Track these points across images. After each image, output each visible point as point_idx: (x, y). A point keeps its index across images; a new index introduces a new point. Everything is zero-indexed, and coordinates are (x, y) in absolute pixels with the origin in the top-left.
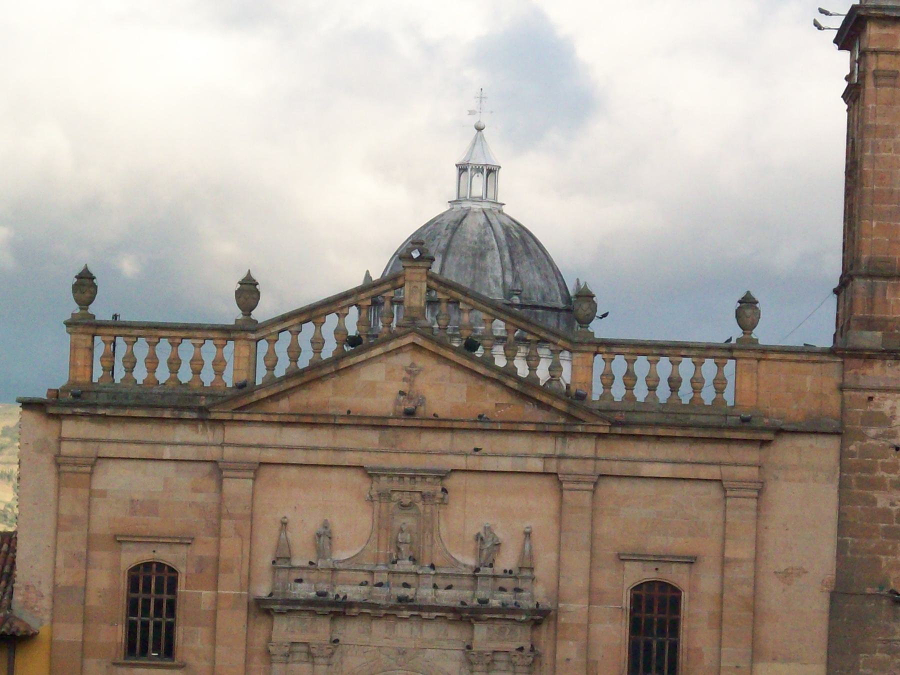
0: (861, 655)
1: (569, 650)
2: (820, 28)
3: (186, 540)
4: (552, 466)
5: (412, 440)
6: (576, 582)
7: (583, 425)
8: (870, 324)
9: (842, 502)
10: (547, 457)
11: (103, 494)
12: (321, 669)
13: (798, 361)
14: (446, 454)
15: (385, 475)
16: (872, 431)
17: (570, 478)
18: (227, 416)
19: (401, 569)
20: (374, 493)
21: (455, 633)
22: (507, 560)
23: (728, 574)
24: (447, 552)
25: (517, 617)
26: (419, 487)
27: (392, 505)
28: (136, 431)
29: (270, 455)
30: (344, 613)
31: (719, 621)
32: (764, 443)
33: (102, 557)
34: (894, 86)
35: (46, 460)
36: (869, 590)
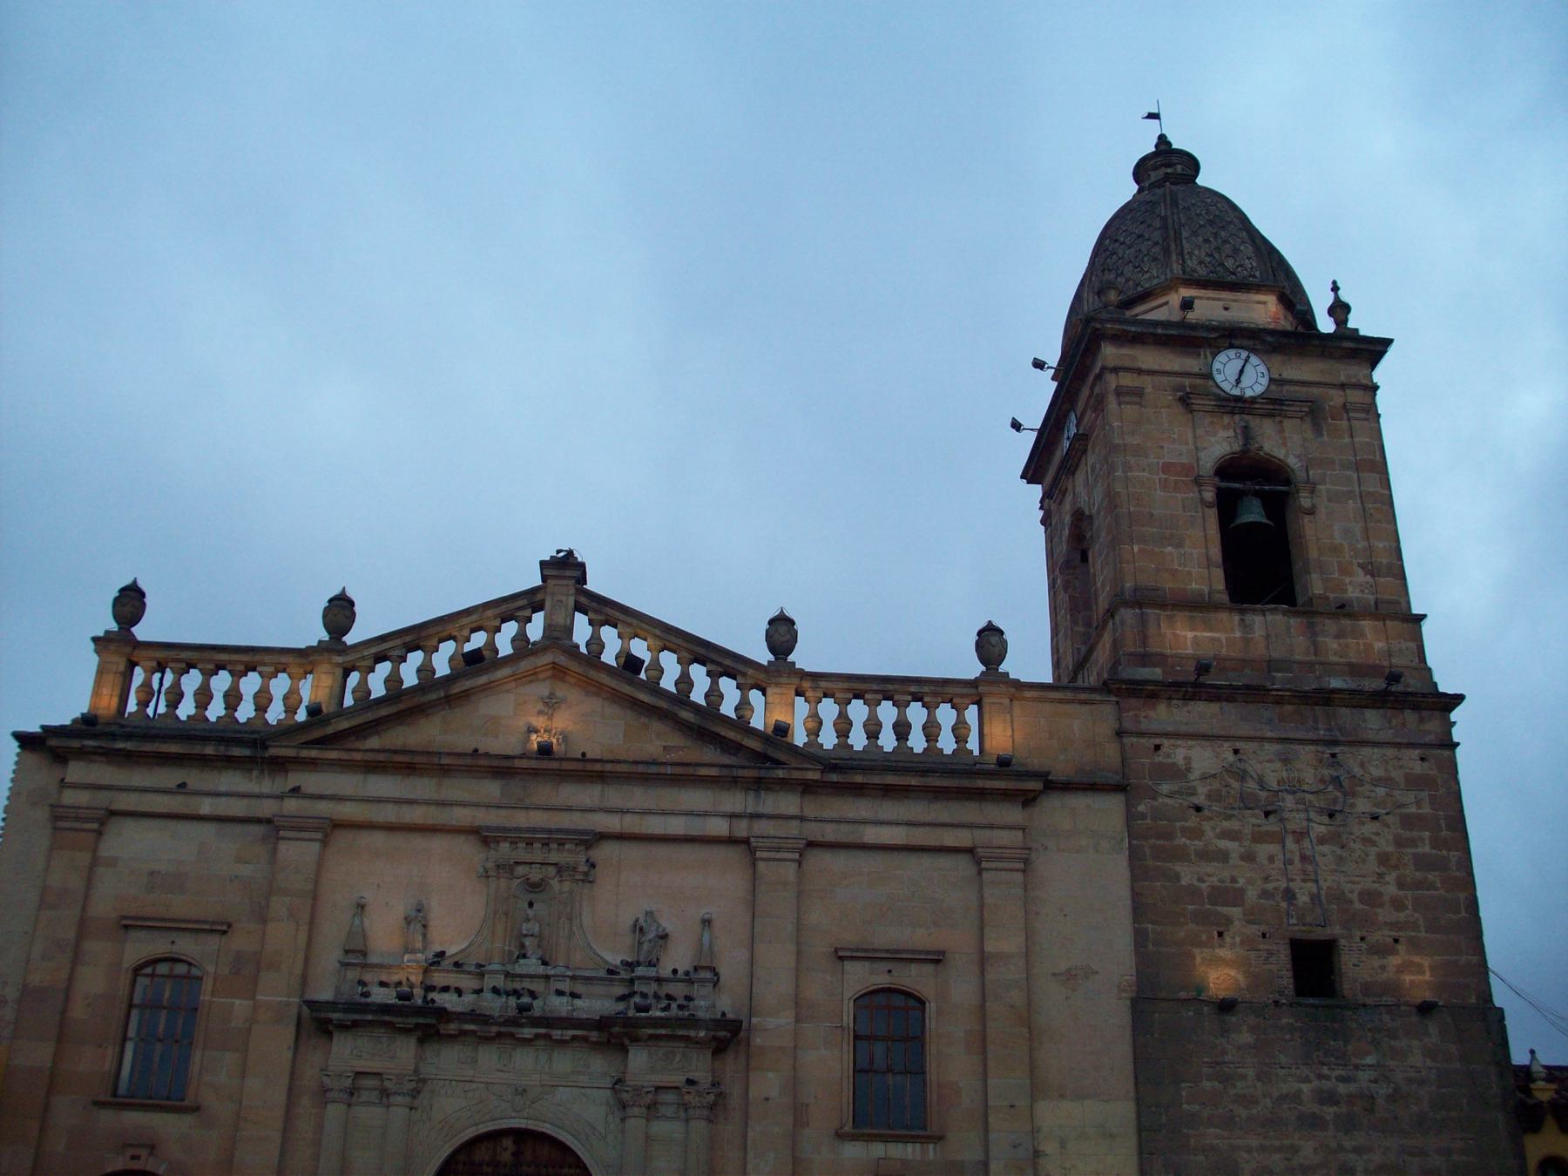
0: (1183, 1085)
1: (768, 1084)
3: (222, 929)
4: (742, 828)
5: (545, 793)
6: (776, 983)
7: (783, 768)
8: (1145, 659)
9: (1135, 876)
10: (733, 816)
11: (113, 863)
12: (399, 1114)
13: (1061, 701)
14: (591, 810)
15: (505, 839)
16: (1165, 788)
18: (291, 753)
19: (524, 971)
20: (490, 865)
21: (599, 1065)
22: (678, 958)
23: (988, 977)
24: (591, 948)
25: (692, 1033)
26: (554, 857)
27: (516, 882)
28: (168, 777)
29: (348, 811)
30: (438, 1032)
31: (981, 1042)
32: (1028, 800)
33: (96, 948)
35: (42, 814)
36: (1183, 995)
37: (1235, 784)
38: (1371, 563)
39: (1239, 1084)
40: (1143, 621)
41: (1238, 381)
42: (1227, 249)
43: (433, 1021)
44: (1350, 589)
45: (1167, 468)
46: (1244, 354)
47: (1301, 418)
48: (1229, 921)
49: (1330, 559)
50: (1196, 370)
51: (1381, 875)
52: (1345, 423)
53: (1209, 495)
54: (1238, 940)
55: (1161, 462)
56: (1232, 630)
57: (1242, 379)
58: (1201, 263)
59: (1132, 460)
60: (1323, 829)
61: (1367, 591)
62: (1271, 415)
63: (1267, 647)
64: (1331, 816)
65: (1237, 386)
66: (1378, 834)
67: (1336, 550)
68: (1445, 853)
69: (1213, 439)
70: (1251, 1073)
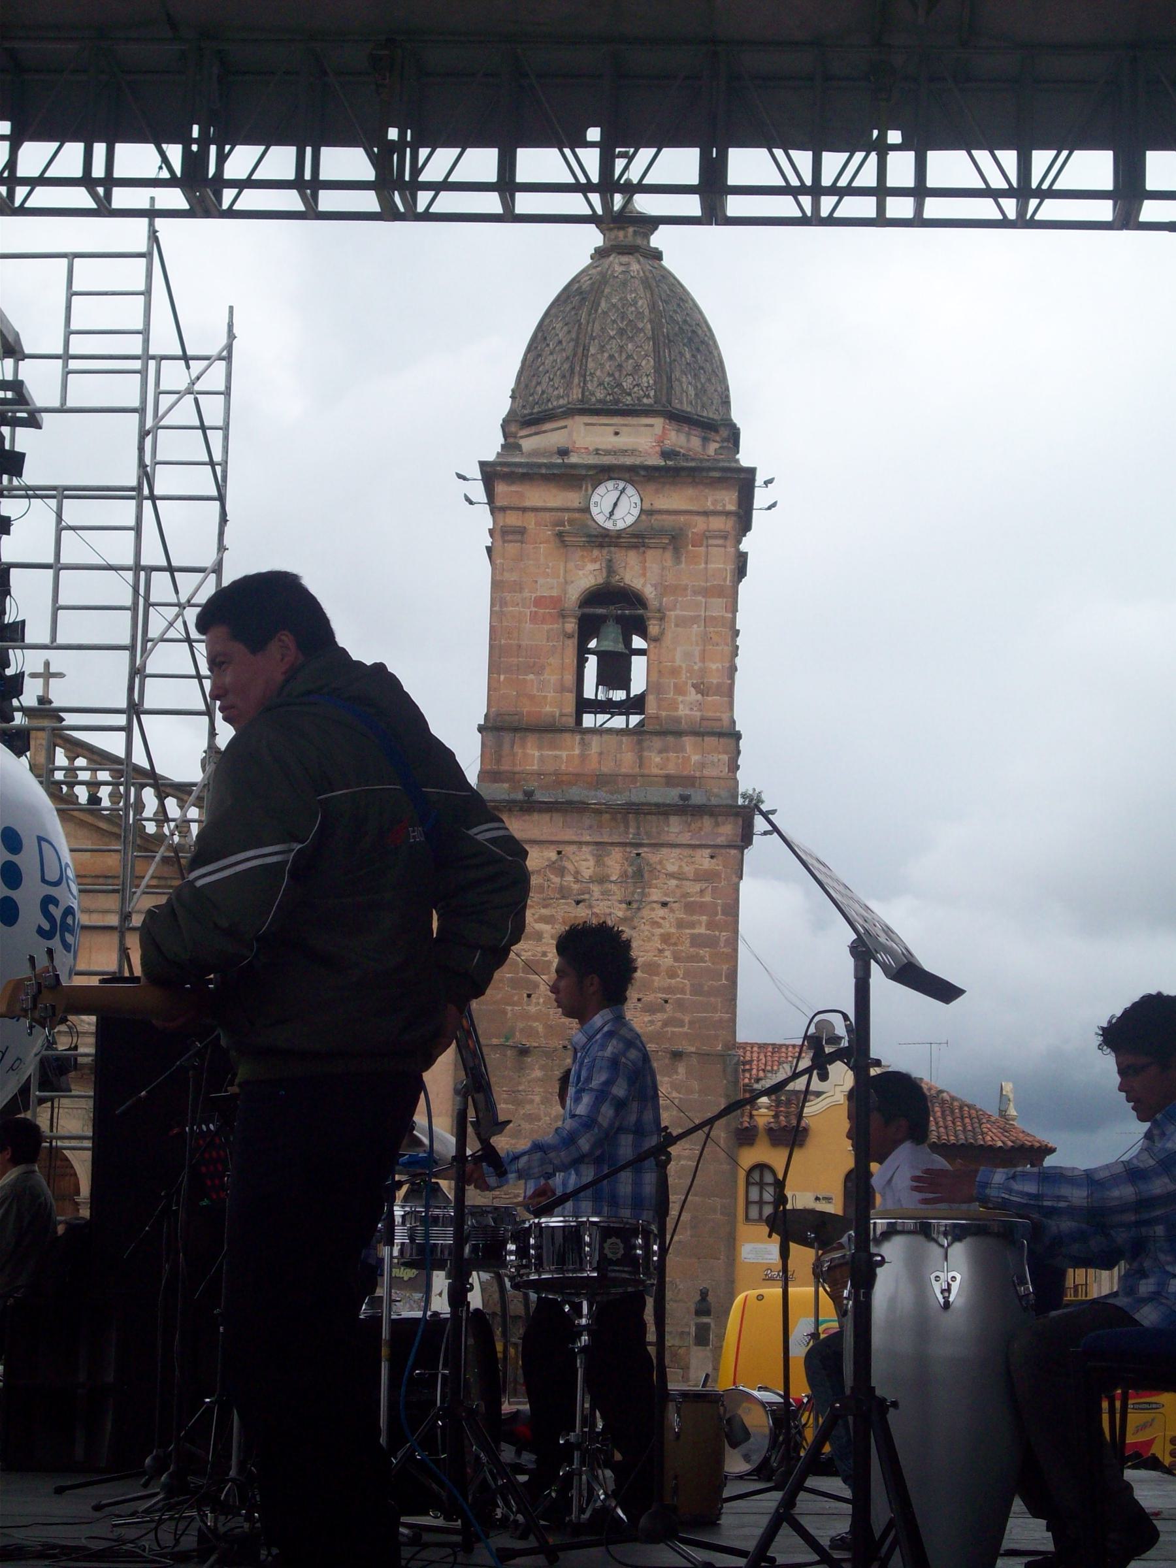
2: (471, 503)
34: (522, 542)
37: (557, 880)
38: (702, 683)
39: (528, 1107)
40: (499, 745)
41: (612, 513)
42: (629, 366)
44: (681, 707)
45: (539, 602)
46: (621, 484)
47: (664, 548)
48: (536, 986)
49: (667, 680)
50: (576, 505)
51: (661, 951)
52: (702, 549)
53: (571, 626)
54: (541, 1000)
55: (534, 595)
56: (573, 748)
57: (615, 512)
58: (601, 384)
59: (508, 596)
60: (620, 914)
61: (695, 709)
62: (635, 547)
63: (600, 763)
64: (630, 903)
65: (610, 518)
66: (664, 918)
67: (675, 672)
68: (717, 933)
69: (581, 573)
70: (537, 1099)
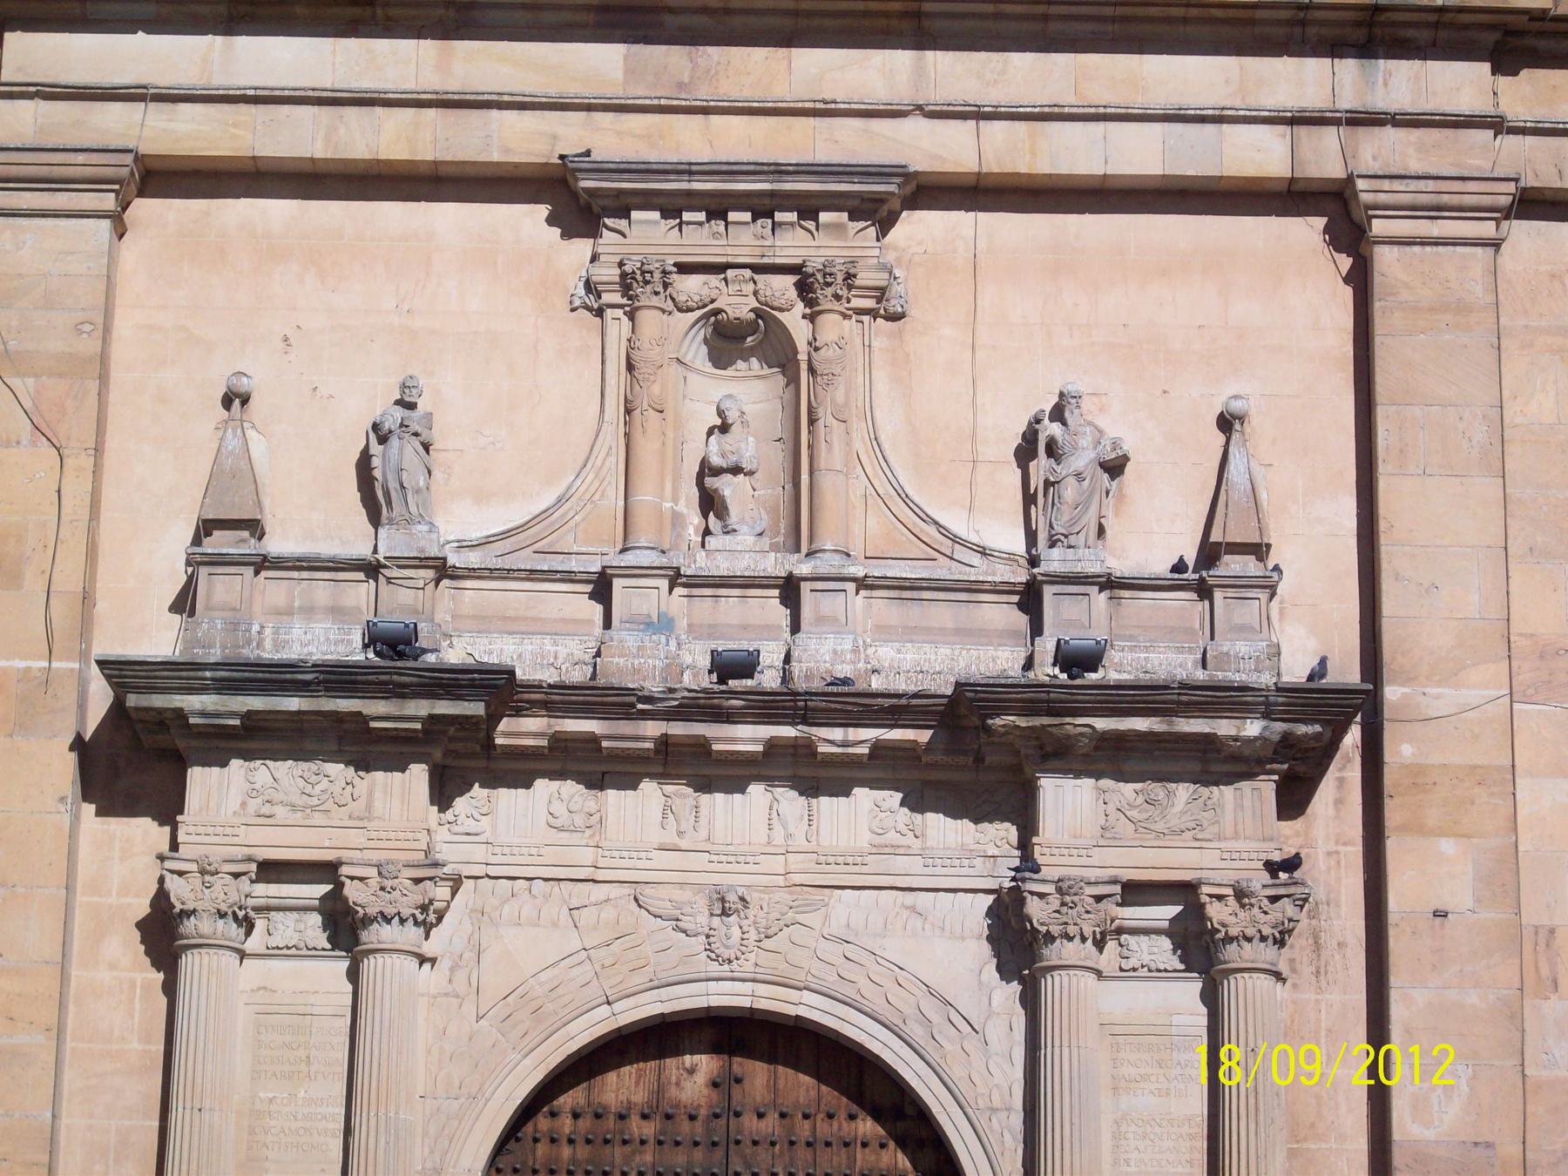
17: (1403, 192)
19: (723, 566)
43: (476, 708)
